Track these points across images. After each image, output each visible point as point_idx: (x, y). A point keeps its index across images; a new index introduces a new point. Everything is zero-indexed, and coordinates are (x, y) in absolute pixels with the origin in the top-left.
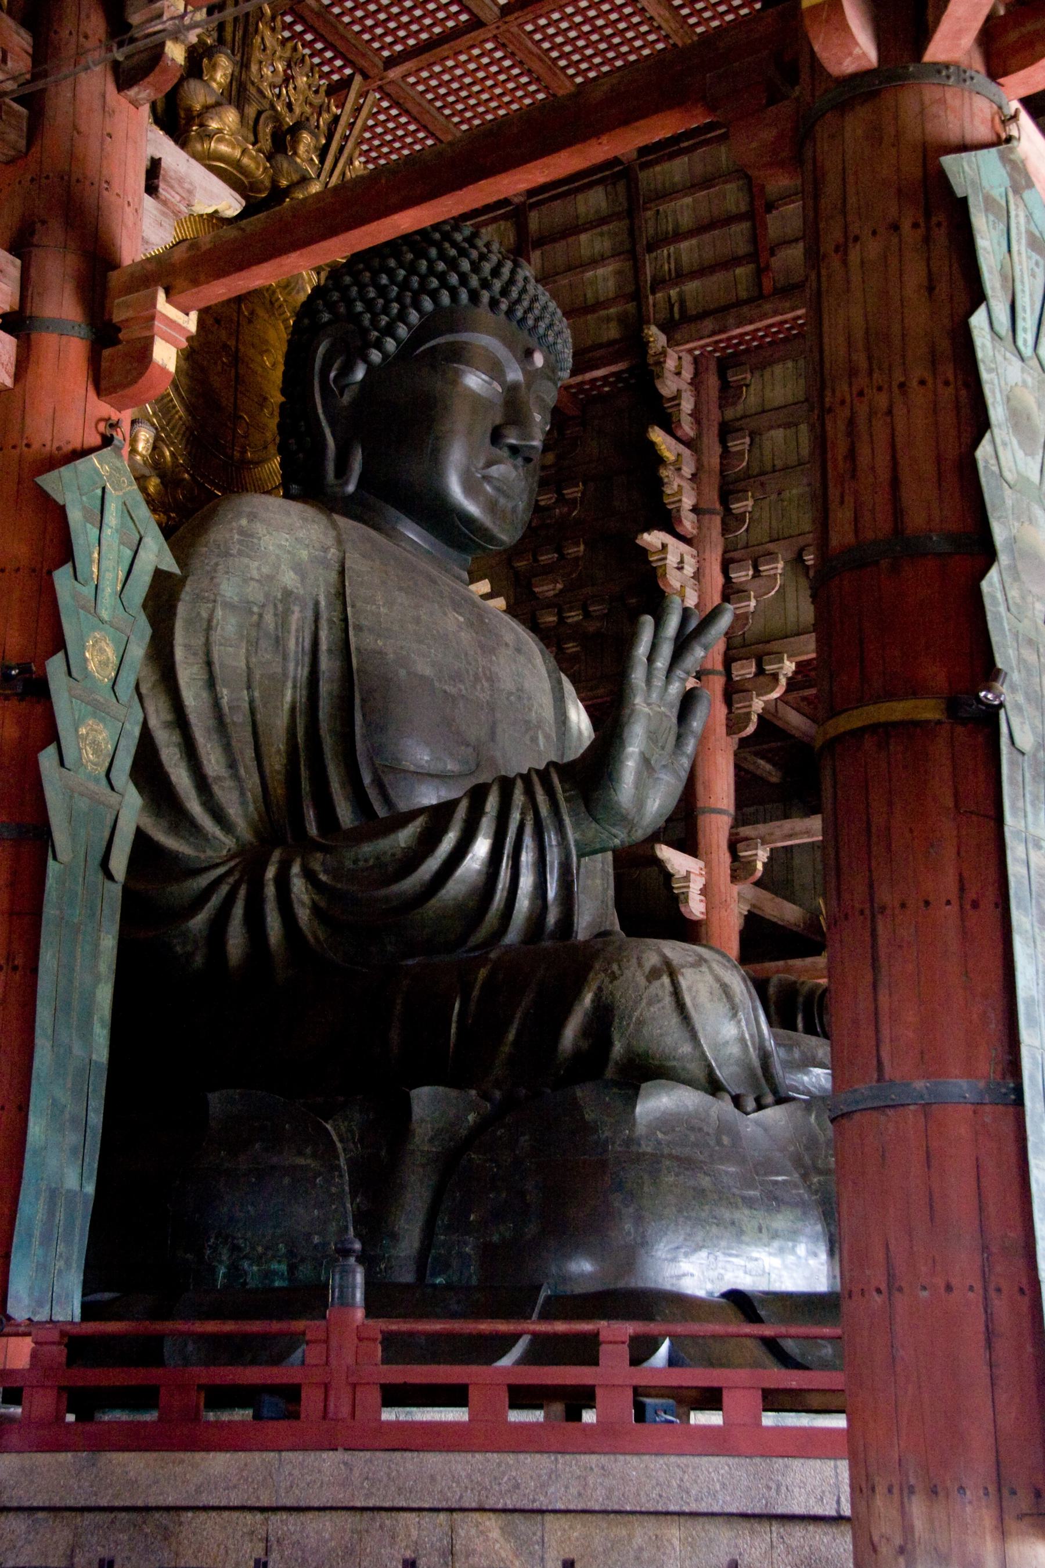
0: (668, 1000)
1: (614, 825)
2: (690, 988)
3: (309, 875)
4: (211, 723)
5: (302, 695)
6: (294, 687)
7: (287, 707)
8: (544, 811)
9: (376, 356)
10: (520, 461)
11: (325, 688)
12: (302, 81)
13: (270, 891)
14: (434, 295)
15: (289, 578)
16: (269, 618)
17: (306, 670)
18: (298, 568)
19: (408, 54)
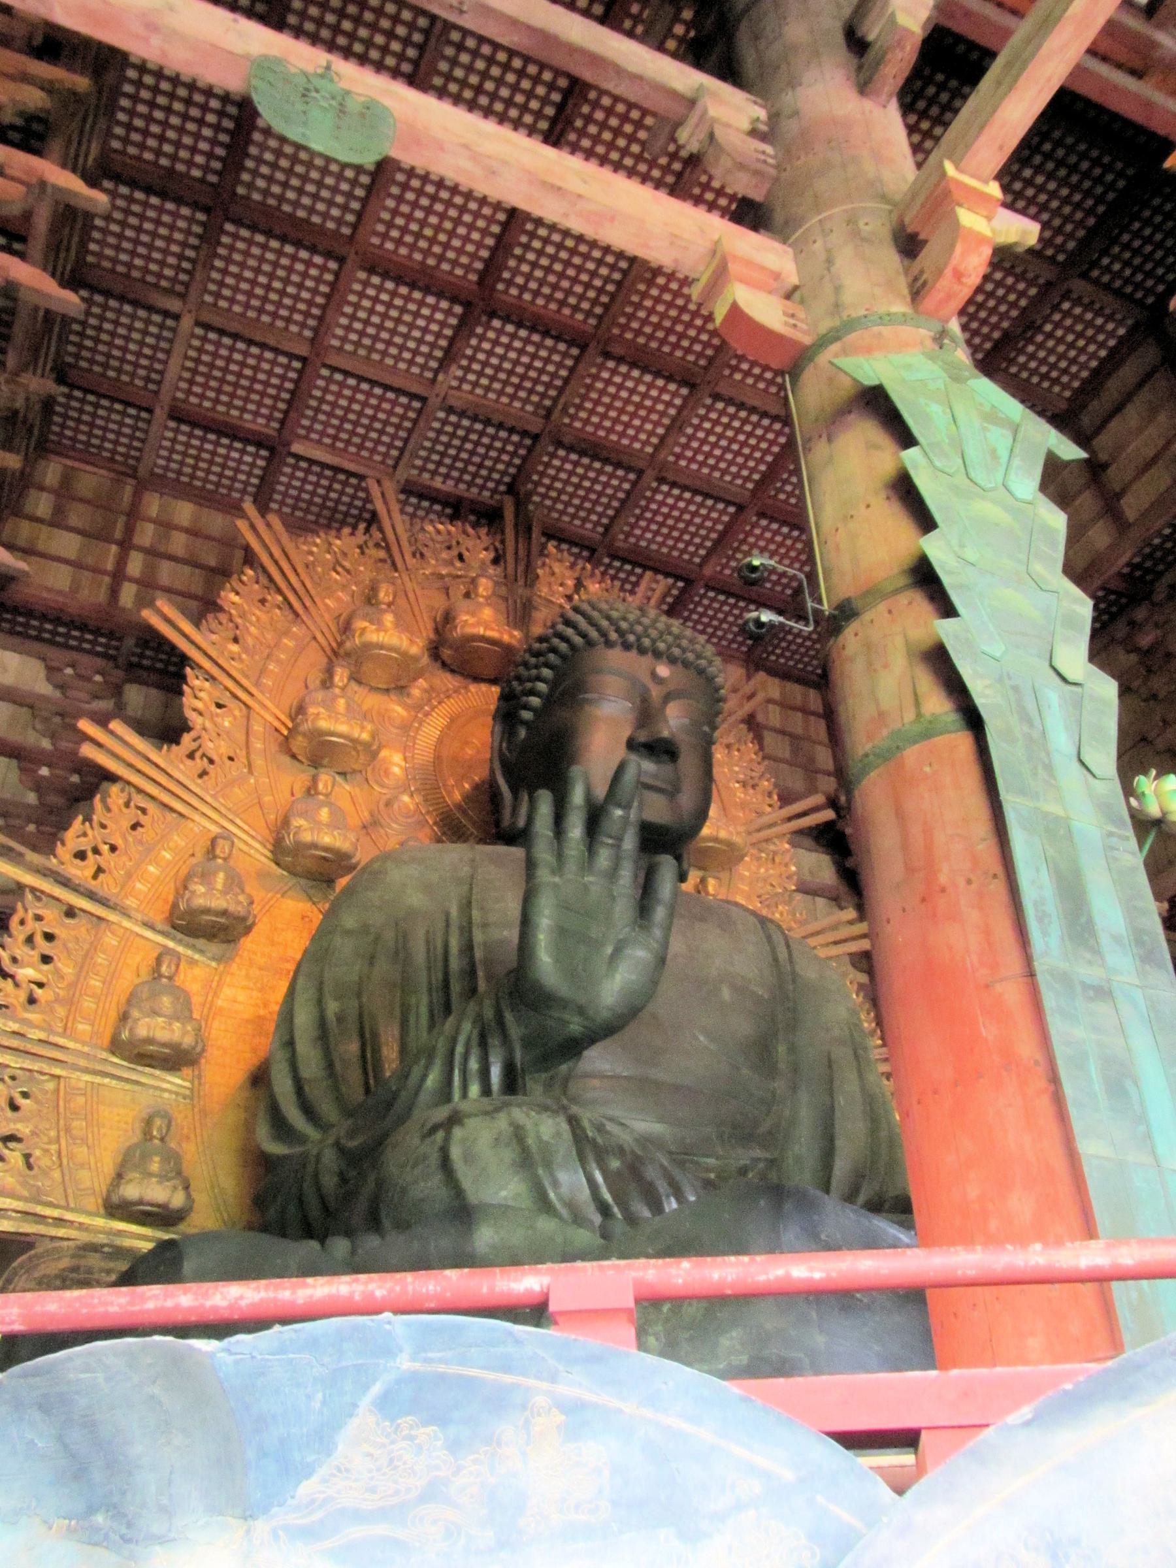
0: (434, 1159)
1: (549, 1007)
2: (464, 1140)
3: (337, 1144)
4: (316, 1033)
5: (438, 997)
6: (430, 990)
7: (424, 1010)
8: (489, 1013)
9: (527, 715)
10: (665, 757)
11: (456, 987)
13: (310, 1169)
14: (554, 650)
15: (416, 899)
16: (389, 935)
17: (440, 976)
18: (428, 889)
19: (711, 552)
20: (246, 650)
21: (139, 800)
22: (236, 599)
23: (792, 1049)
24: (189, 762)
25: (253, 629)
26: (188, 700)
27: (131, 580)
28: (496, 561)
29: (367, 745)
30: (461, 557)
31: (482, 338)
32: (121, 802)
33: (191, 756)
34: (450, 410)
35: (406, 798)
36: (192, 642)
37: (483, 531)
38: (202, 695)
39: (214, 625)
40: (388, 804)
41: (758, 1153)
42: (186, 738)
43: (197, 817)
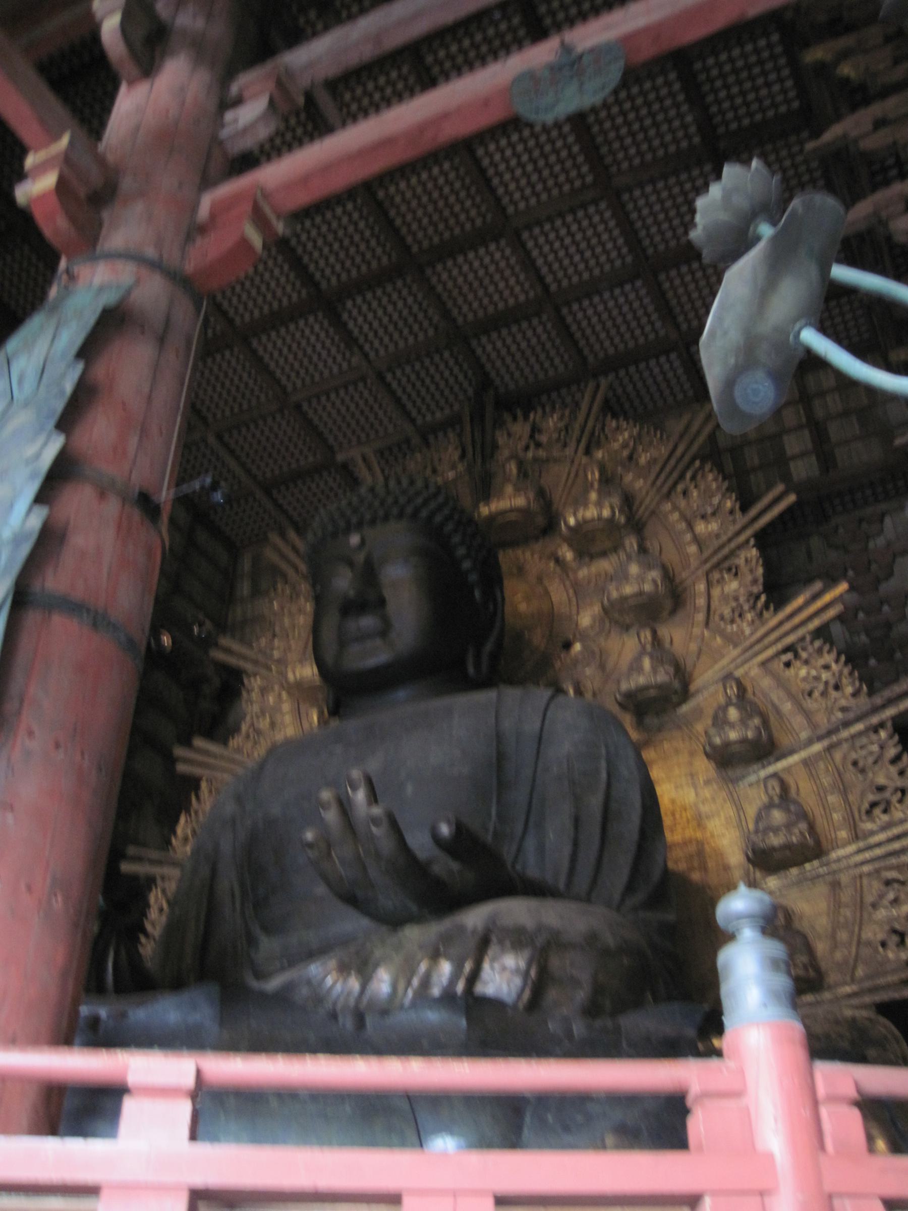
28: (463, 456)
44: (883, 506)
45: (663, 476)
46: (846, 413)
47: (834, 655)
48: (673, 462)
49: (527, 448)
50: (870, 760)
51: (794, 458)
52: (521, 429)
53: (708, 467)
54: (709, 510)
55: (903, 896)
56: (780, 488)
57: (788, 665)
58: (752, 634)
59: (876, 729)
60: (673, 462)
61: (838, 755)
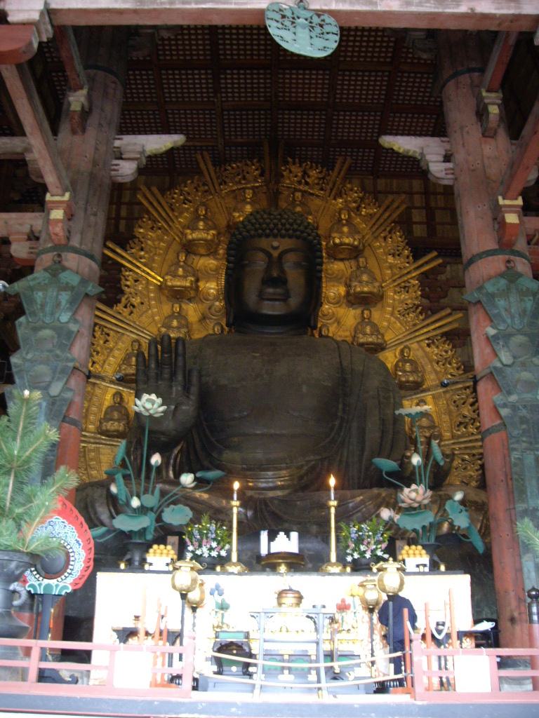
12: (313, 173)
20: (147, 252)
21: (105, 330)
22: (142, 230)
23: (344, 404)
24: (125, 310)
25: (149, 242)
26: (123, 282)
27: (123, 219)
28: (262, 175)
29: (191, 288)
30: (244, 178)
31: (226, 79)
32: (99, 333)
33: (126, 307)
34: (228, 111)
35: (217, 303)
36: (122, 257)
37: (255, 160)
38: (130, 278)
39: (132, 245)
40: (210, 308)
41: (312, 457)
42: (123, 300)
43: (128, 333)
44: (448, 259)
45: (376, 226)
46: (444, 209)
47: (451, 347)
48: (382, 220)
49: (300, 182)
50: (462, 401)
51: (416, 223)
52: (297, 170)
53: (398, 228)
54: (398, 253)
55: (469, 468)
56: (435, 254)
57: (429, 345)
58: (415, 325)
59: (466, 388)
60: (382, 220)
61: (448, 395)
